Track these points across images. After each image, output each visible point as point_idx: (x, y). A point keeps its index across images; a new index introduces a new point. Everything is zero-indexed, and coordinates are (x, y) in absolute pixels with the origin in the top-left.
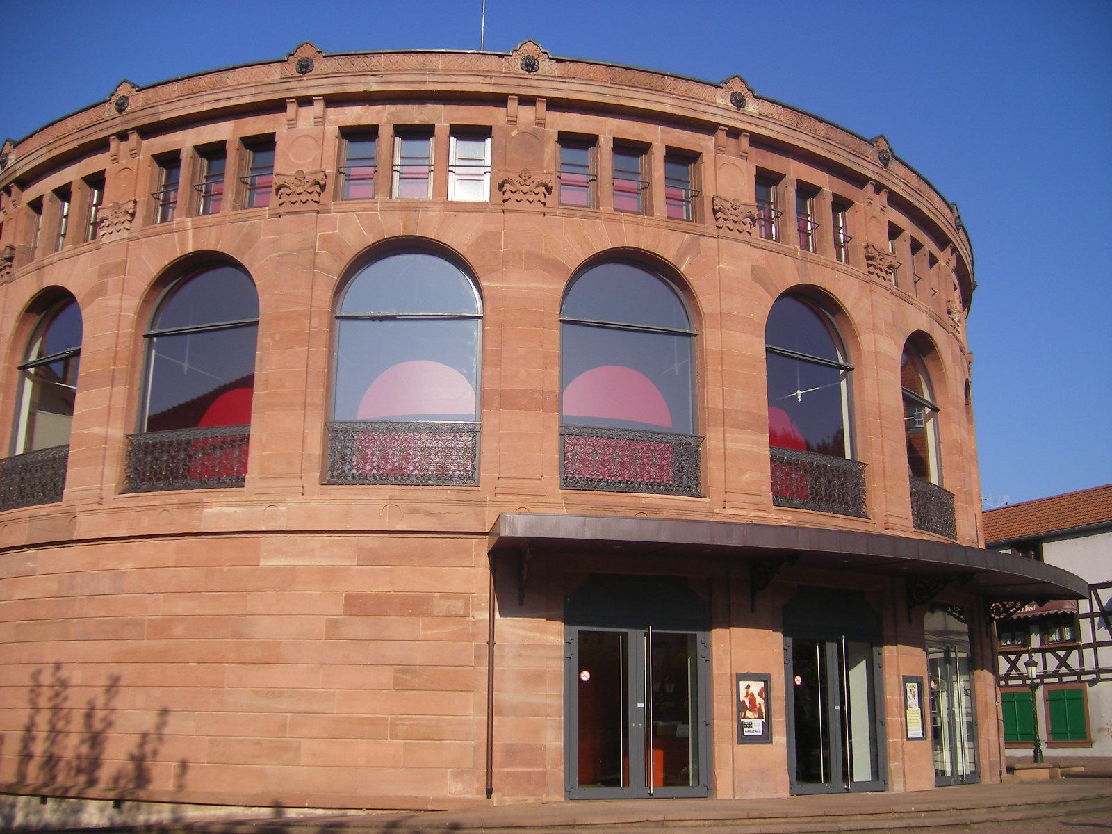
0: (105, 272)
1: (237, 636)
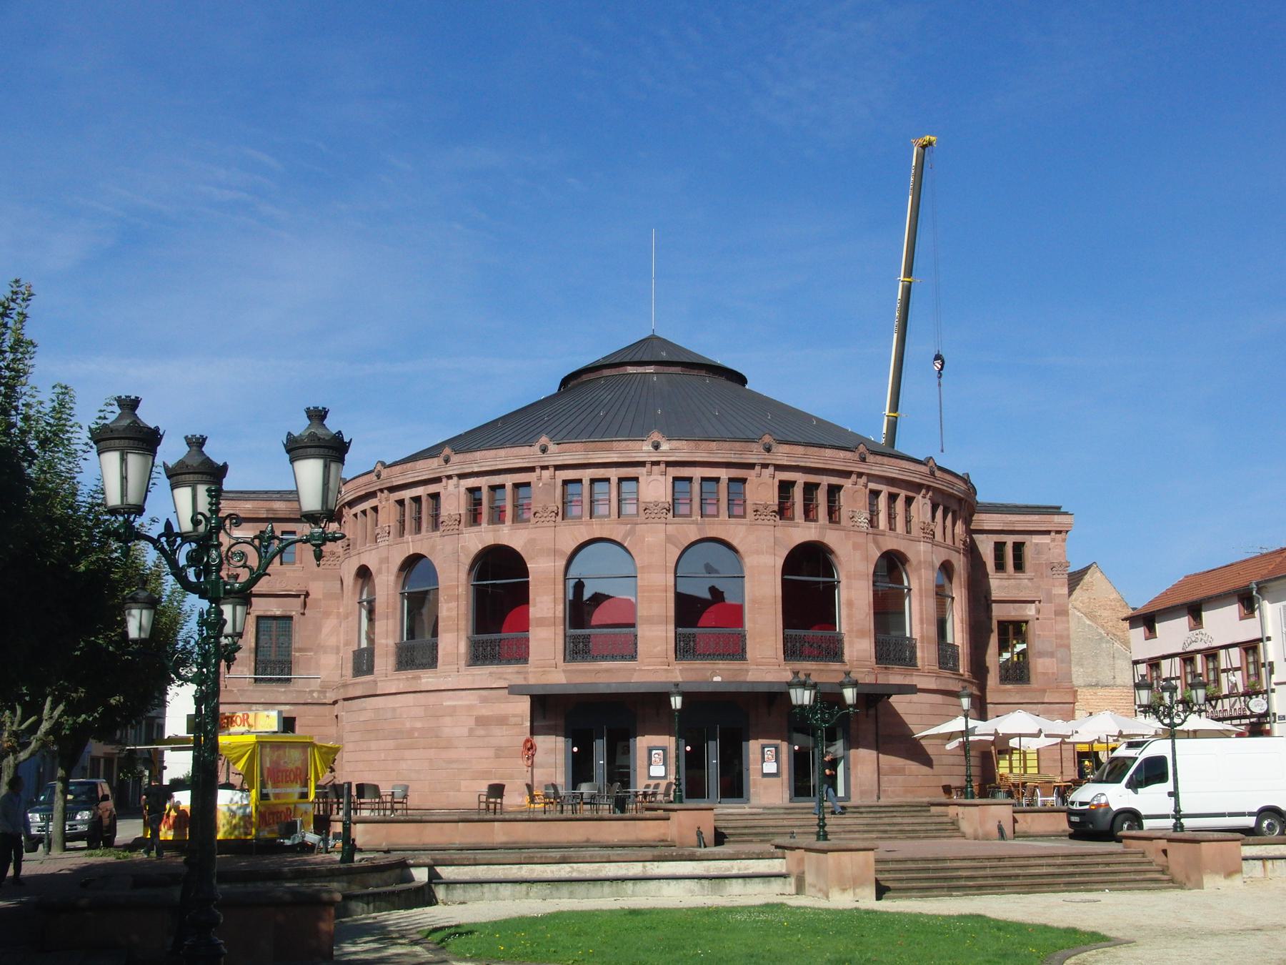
0: (381, 561)
1: (437, 737)
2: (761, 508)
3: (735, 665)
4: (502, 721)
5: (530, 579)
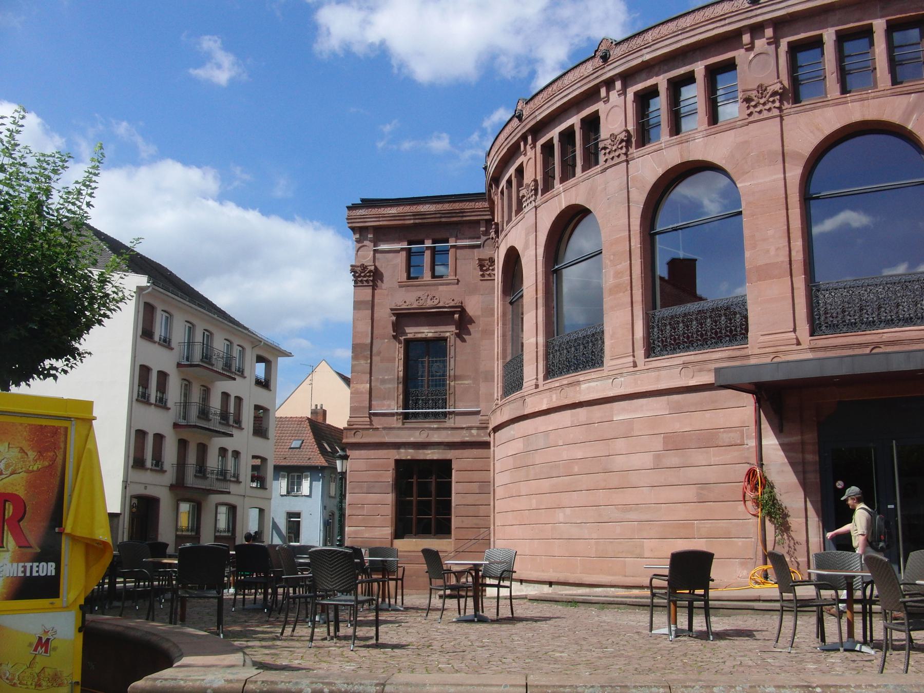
4: (707, 440)
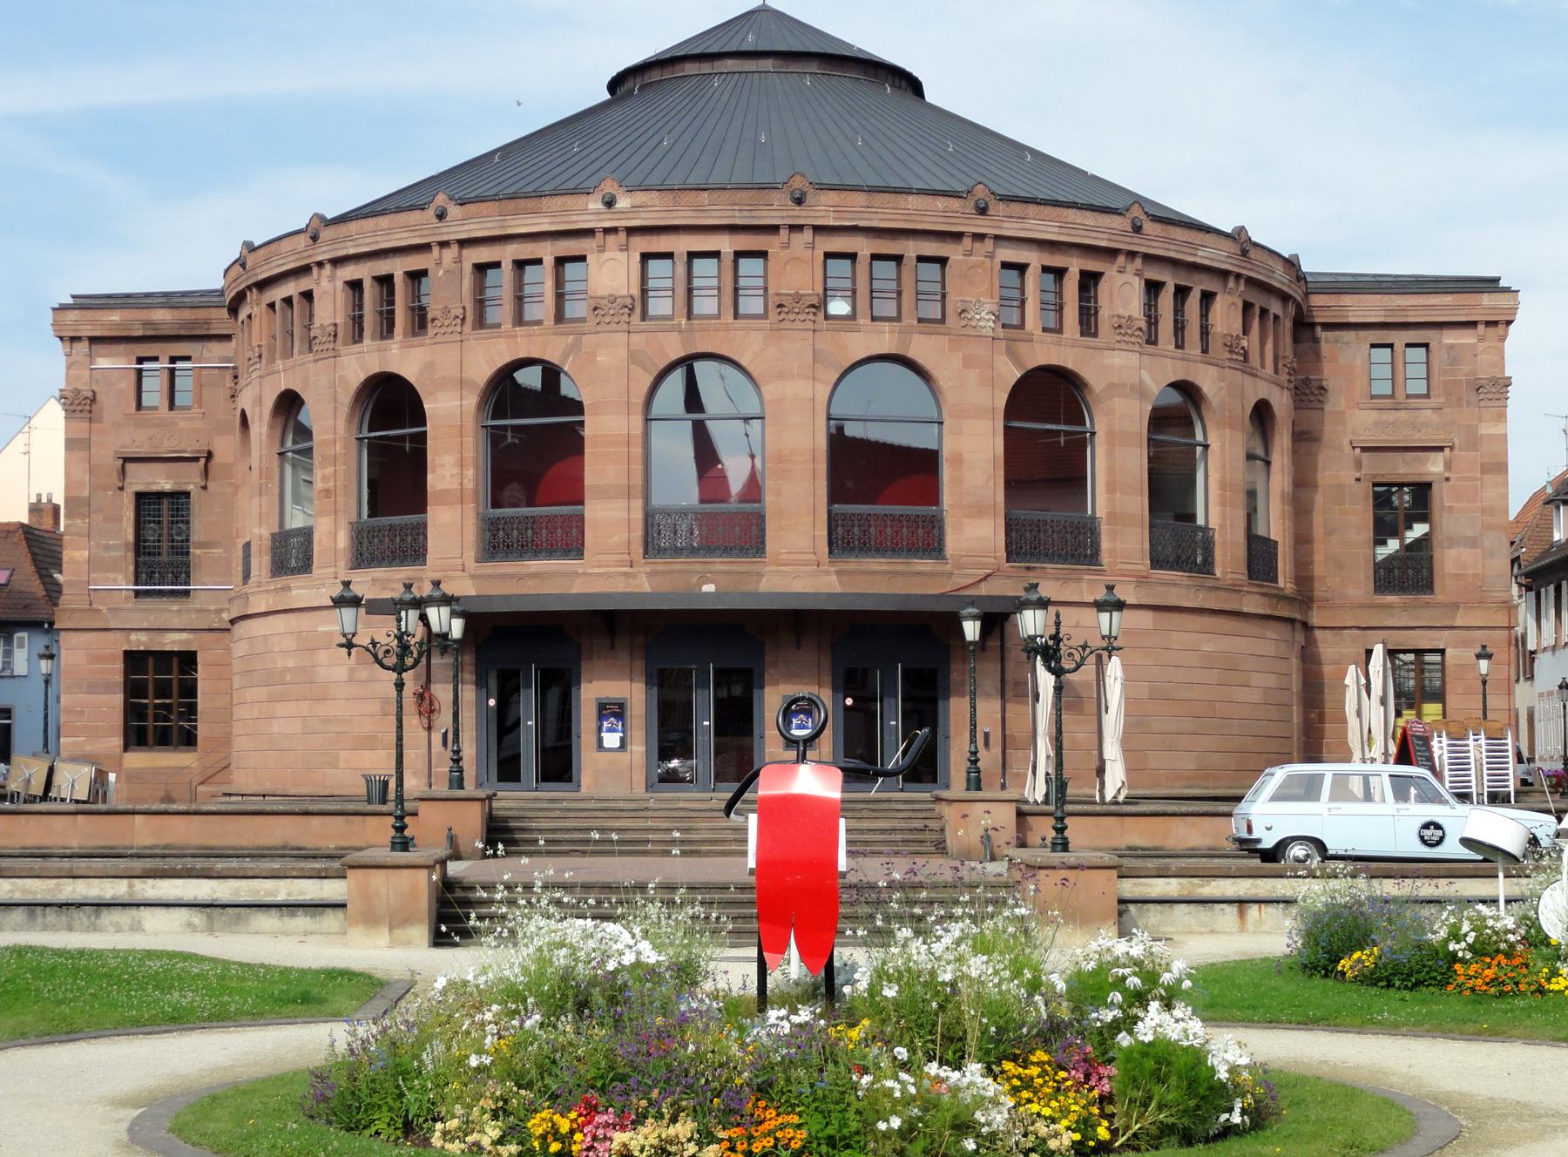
2: (787, 302)
3: (740, 565)
5: (428, 428)
